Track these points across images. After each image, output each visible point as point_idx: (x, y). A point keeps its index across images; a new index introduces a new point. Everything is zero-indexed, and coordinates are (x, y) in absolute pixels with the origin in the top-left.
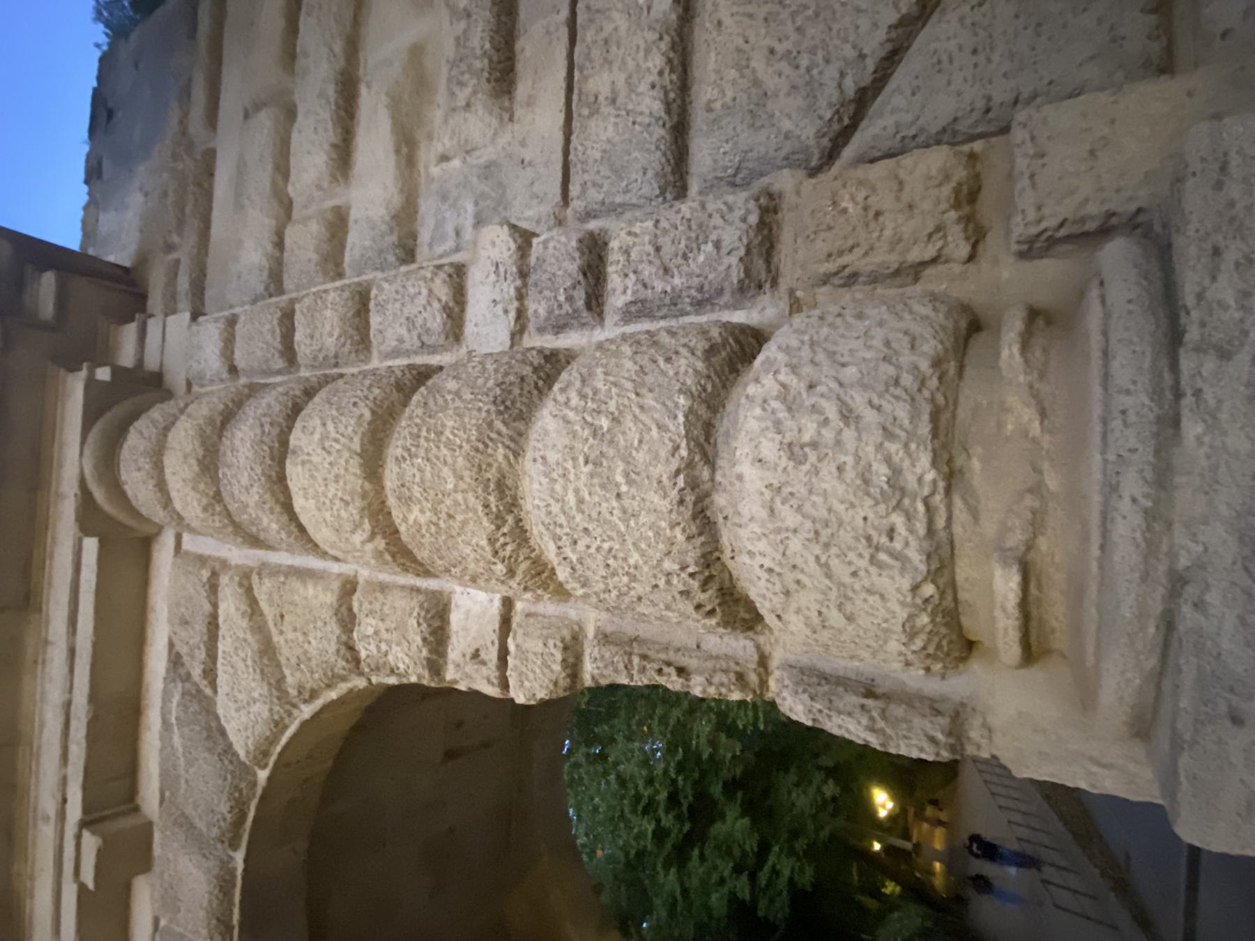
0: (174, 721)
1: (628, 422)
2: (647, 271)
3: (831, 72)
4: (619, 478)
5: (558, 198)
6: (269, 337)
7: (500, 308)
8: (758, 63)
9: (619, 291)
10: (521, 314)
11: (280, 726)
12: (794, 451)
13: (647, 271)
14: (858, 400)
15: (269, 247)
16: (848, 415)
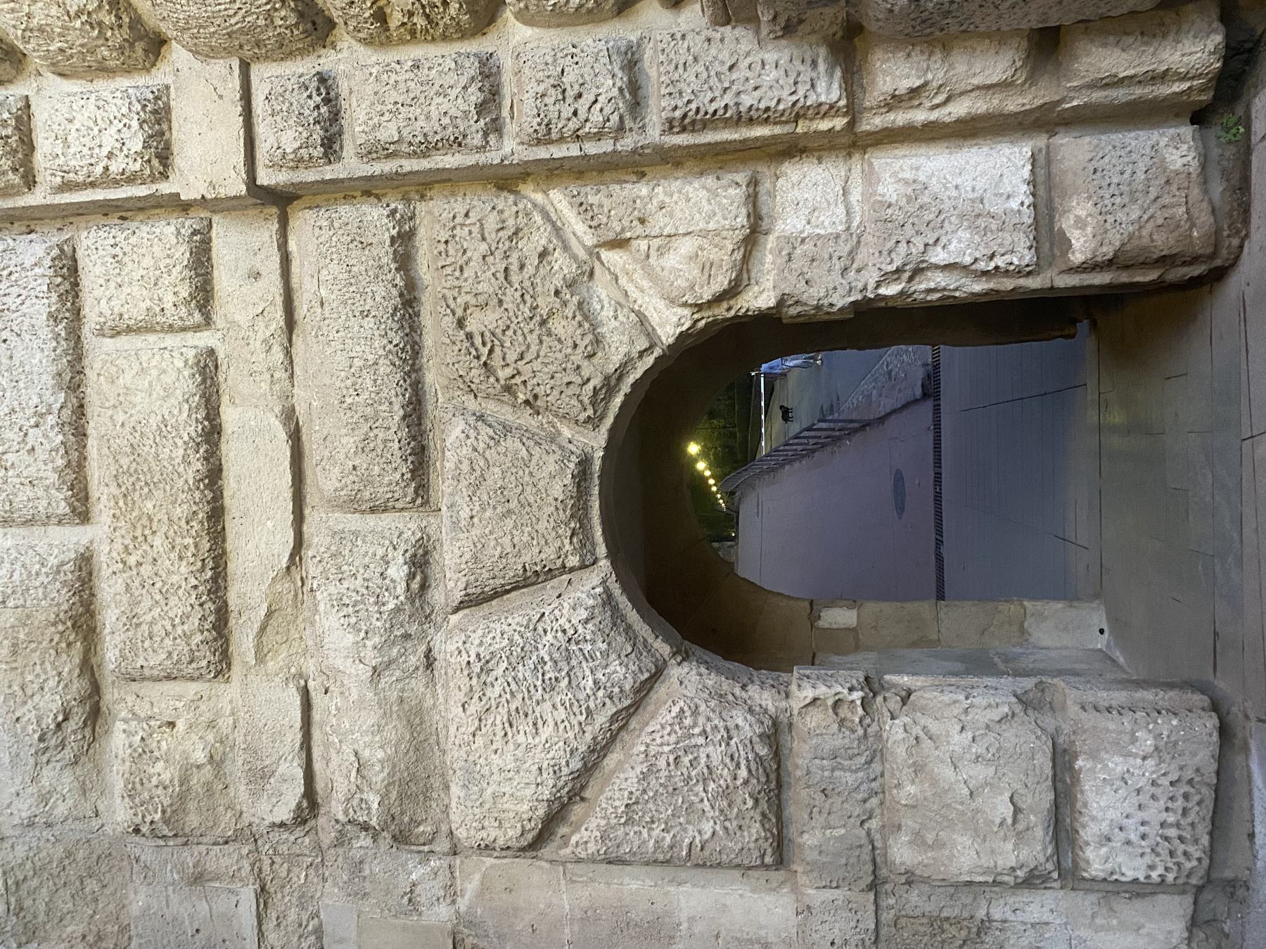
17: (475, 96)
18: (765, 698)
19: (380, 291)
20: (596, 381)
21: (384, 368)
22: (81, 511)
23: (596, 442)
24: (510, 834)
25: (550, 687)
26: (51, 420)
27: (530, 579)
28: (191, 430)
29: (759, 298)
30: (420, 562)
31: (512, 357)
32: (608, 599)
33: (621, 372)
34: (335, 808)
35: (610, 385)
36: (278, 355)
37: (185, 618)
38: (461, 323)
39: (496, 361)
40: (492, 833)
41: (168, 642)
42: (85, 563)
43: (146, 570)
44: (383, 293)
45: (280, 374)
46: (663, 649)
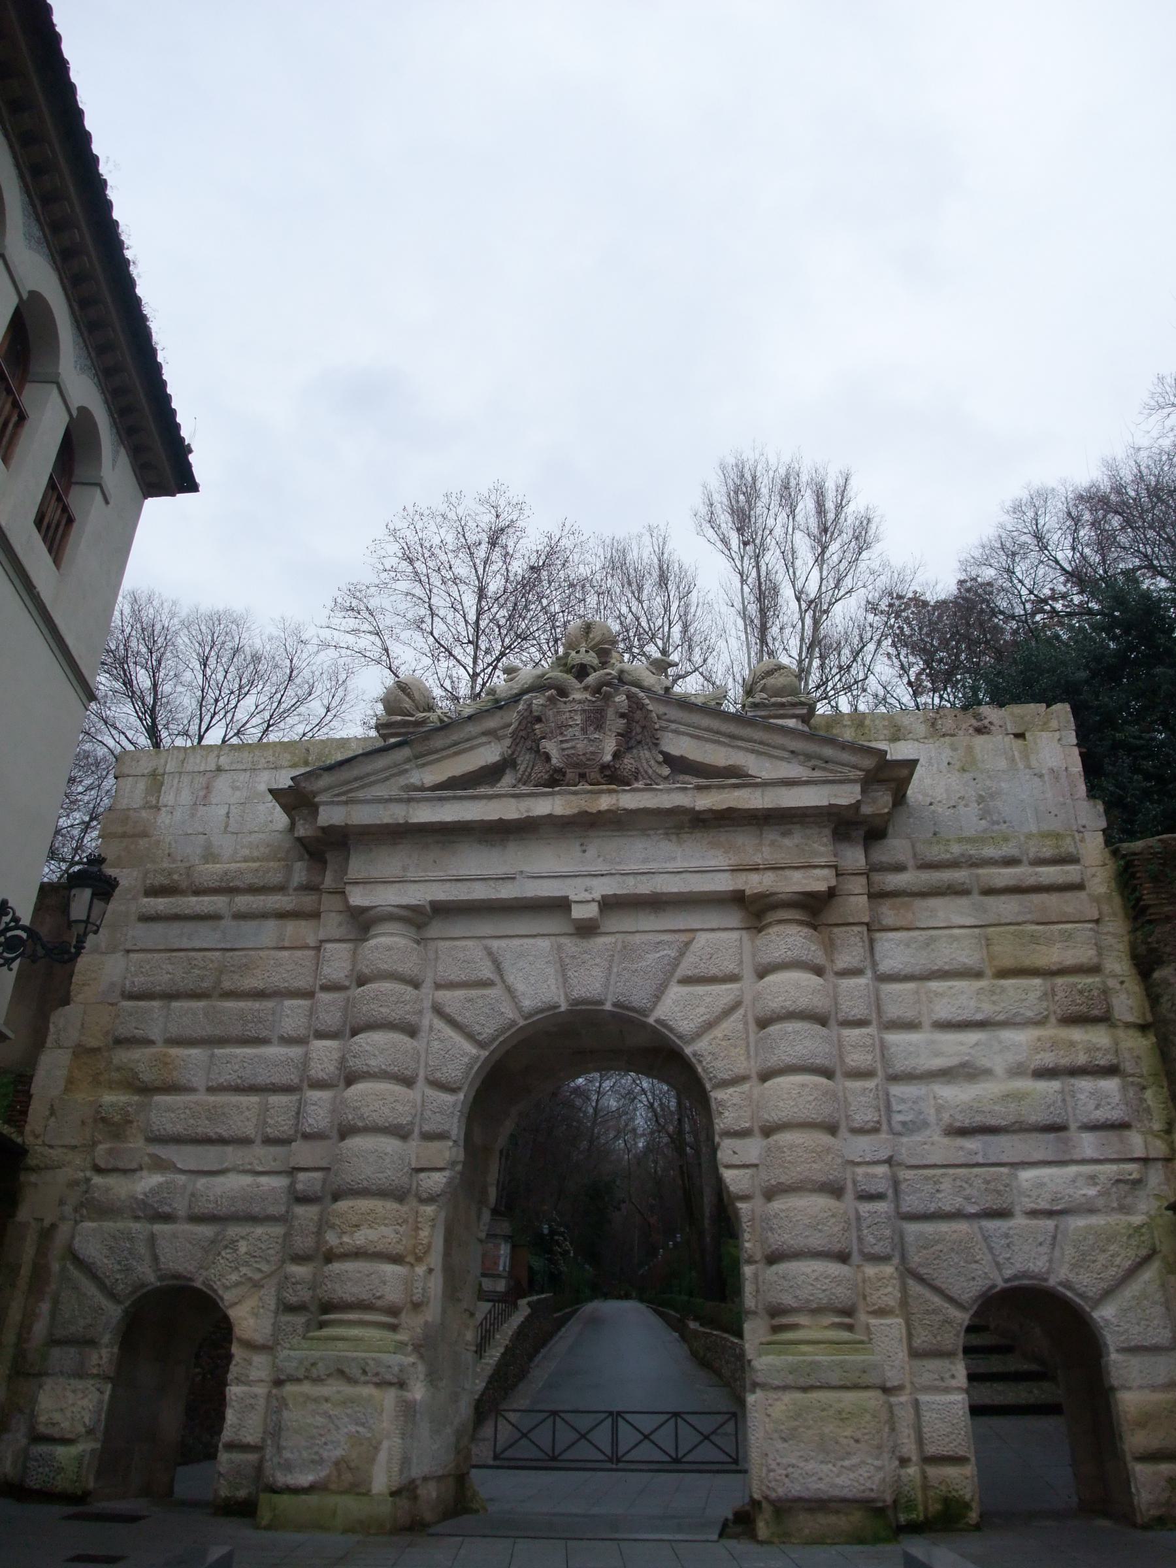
0: (662, 953)
1: (820, 1234)
2: (869, 1220)
3: (931, 1271)
4: (807, 1233)
5: (909, 1164)
6: (853, 1013)
7: (862, 1154)
8: (939, 1247)
9: (865, 1208)
10: (859, 1164)
11: (680, 1037)
12: (817, 1279)
13: (869, 1220)
14: (827, 1293)
15: (903, 973)
16: (824, 1291)
17: (301, 1253)
18: (106, 1339)
19: (257, 1209)
20: (215, 1287)
21: (233, 1209)
22: (211, 1090)
23: (198, 1284)
24: (77, 1244)
25: (119, 1263)
26: (239, 1081)
27: (155, 1258)
28: (225, 1134)
29: (235, 1349)
30: (167, 1218)
31: (228, 1256)
32: (143, 1285)
33: (217, 1294)
34: (97, 1180)
35: (215, 1291)
36: (249, 1167)
37: (165, 1129)
38: (242, 1238)
39: (228, 1251)
40: (77, 1239)
41: (158, 1123)
42: (188, 1090)
43: (182, 1116)
44: (256, 1209)
45: (241, 1168)
46: (128, 1303)
